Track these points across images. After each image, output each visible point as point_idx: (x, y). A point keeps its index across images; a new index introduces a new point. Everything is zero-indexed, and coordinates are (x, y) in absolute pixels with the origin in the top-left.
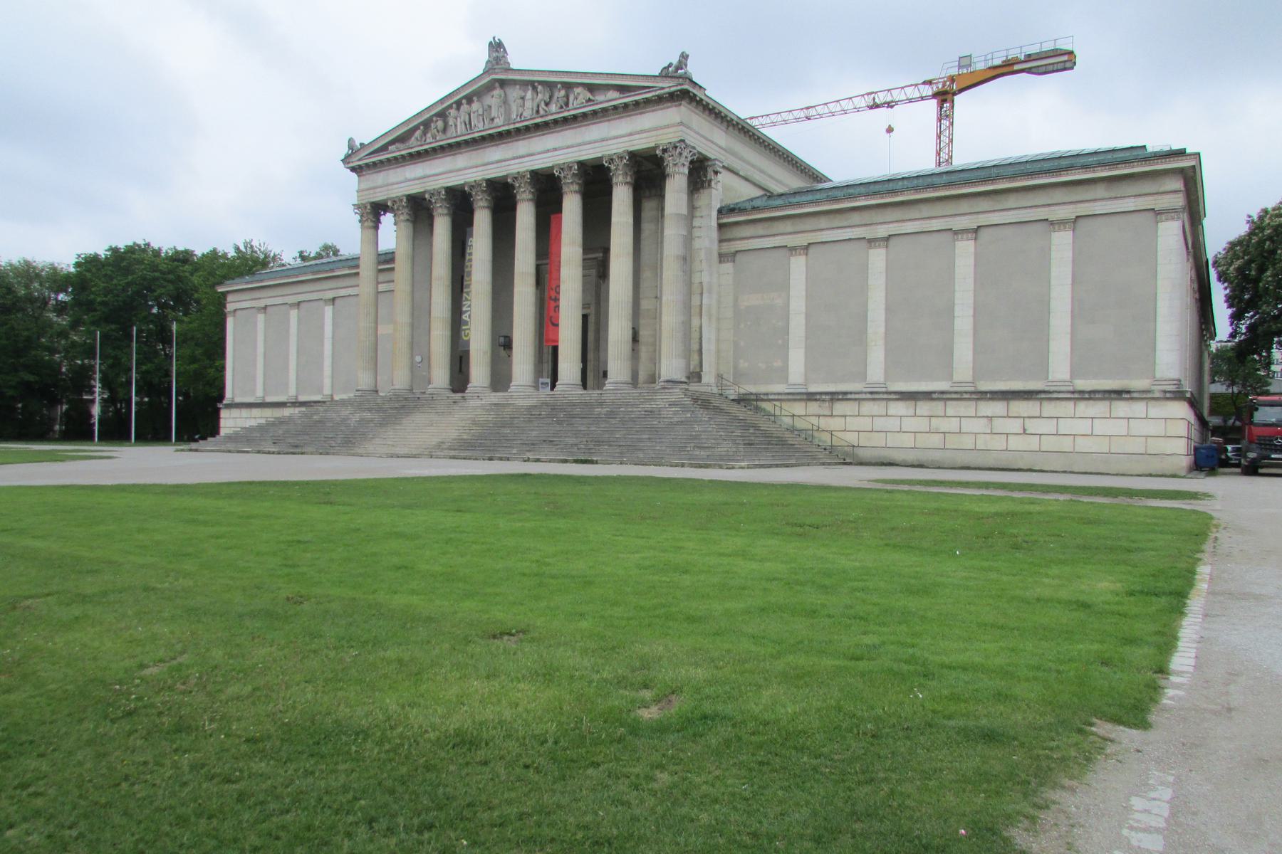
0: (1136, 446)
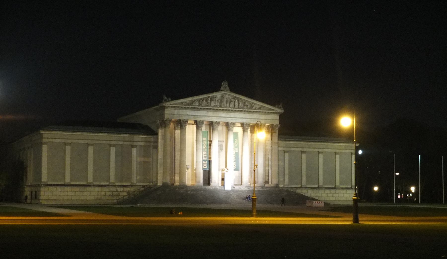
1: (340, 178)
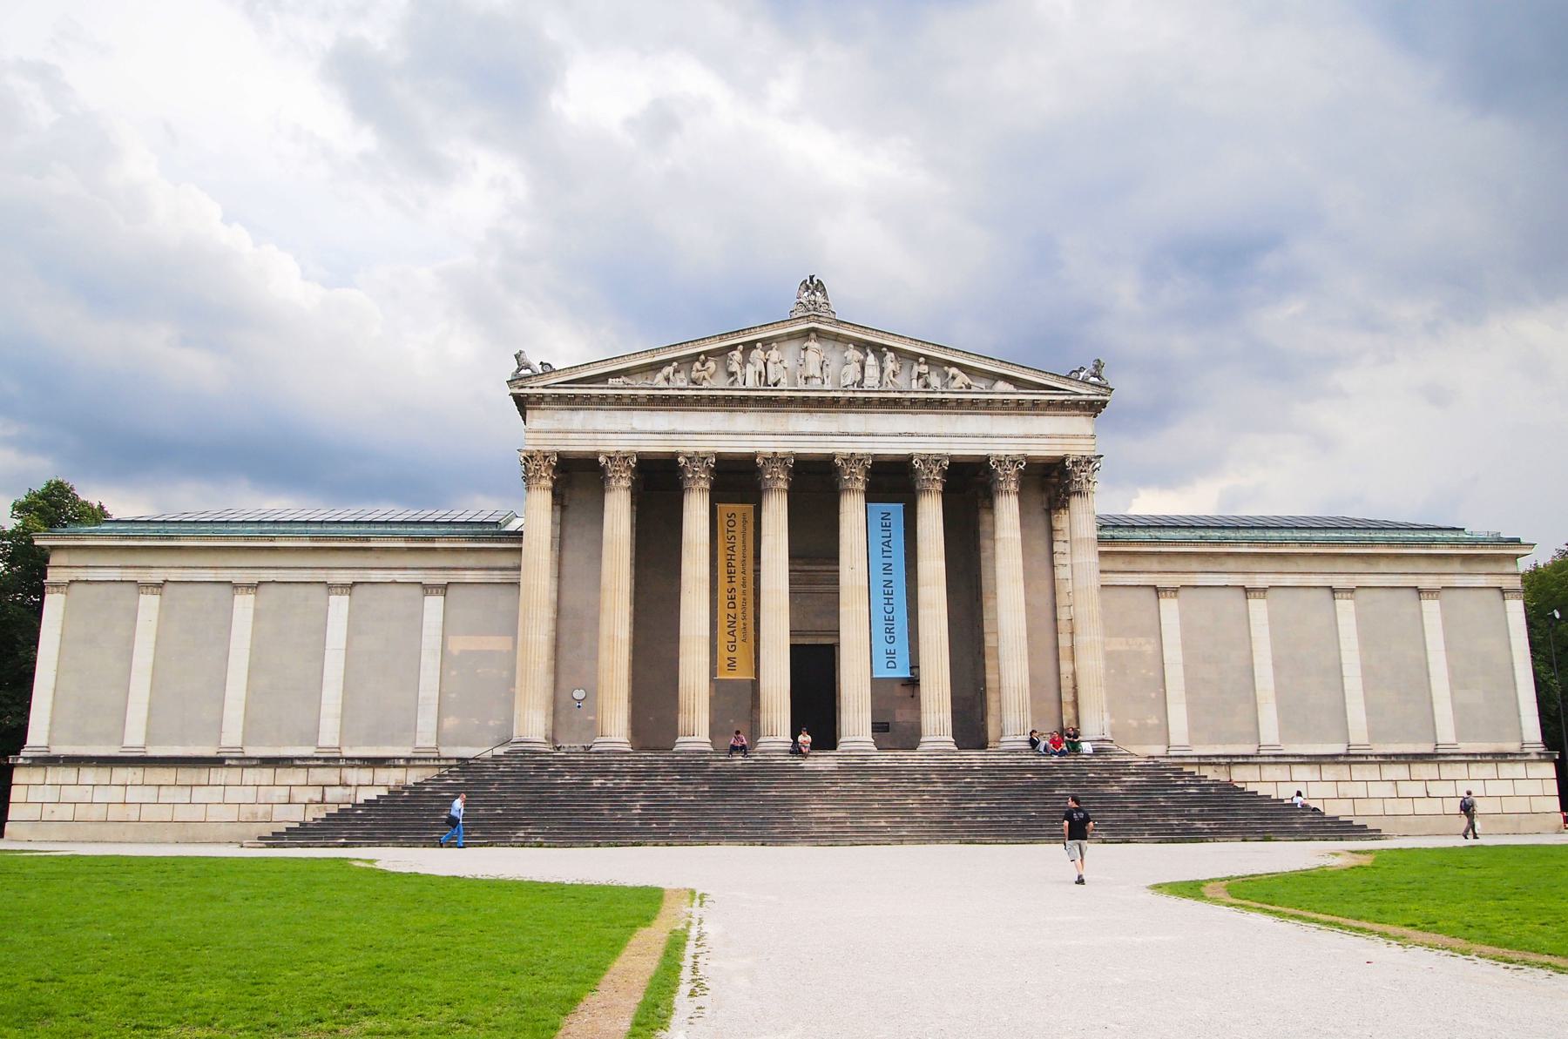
0: (1522, 805)
1: (1460, 711)
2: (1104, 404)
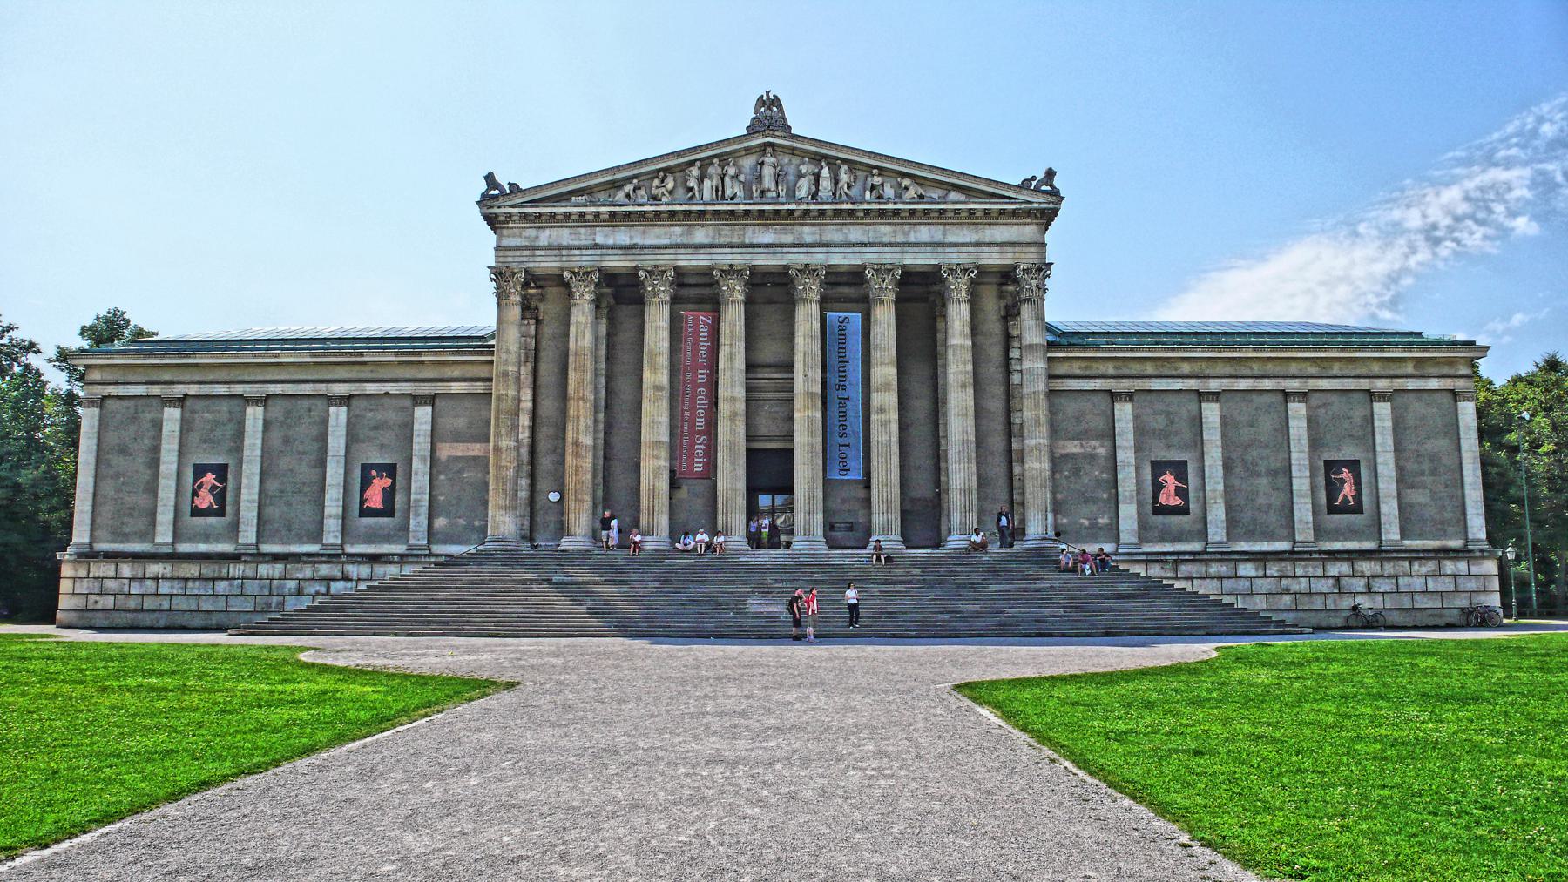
2: (1055, 212)
